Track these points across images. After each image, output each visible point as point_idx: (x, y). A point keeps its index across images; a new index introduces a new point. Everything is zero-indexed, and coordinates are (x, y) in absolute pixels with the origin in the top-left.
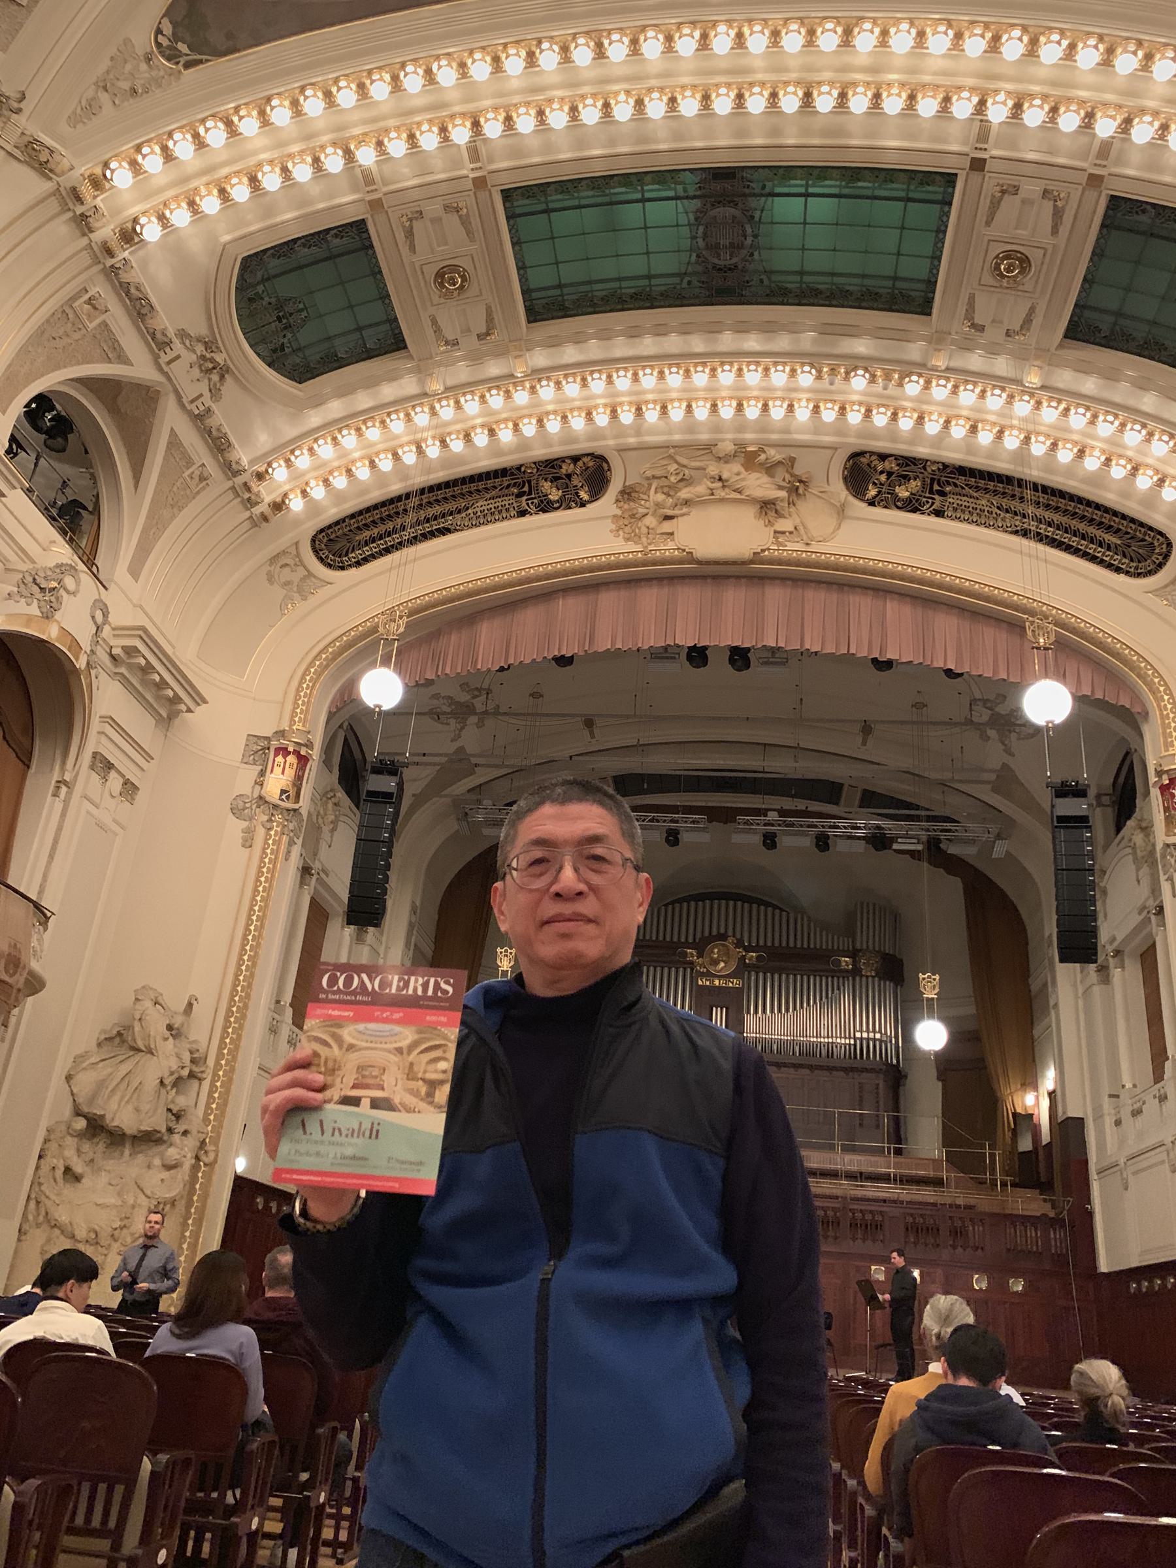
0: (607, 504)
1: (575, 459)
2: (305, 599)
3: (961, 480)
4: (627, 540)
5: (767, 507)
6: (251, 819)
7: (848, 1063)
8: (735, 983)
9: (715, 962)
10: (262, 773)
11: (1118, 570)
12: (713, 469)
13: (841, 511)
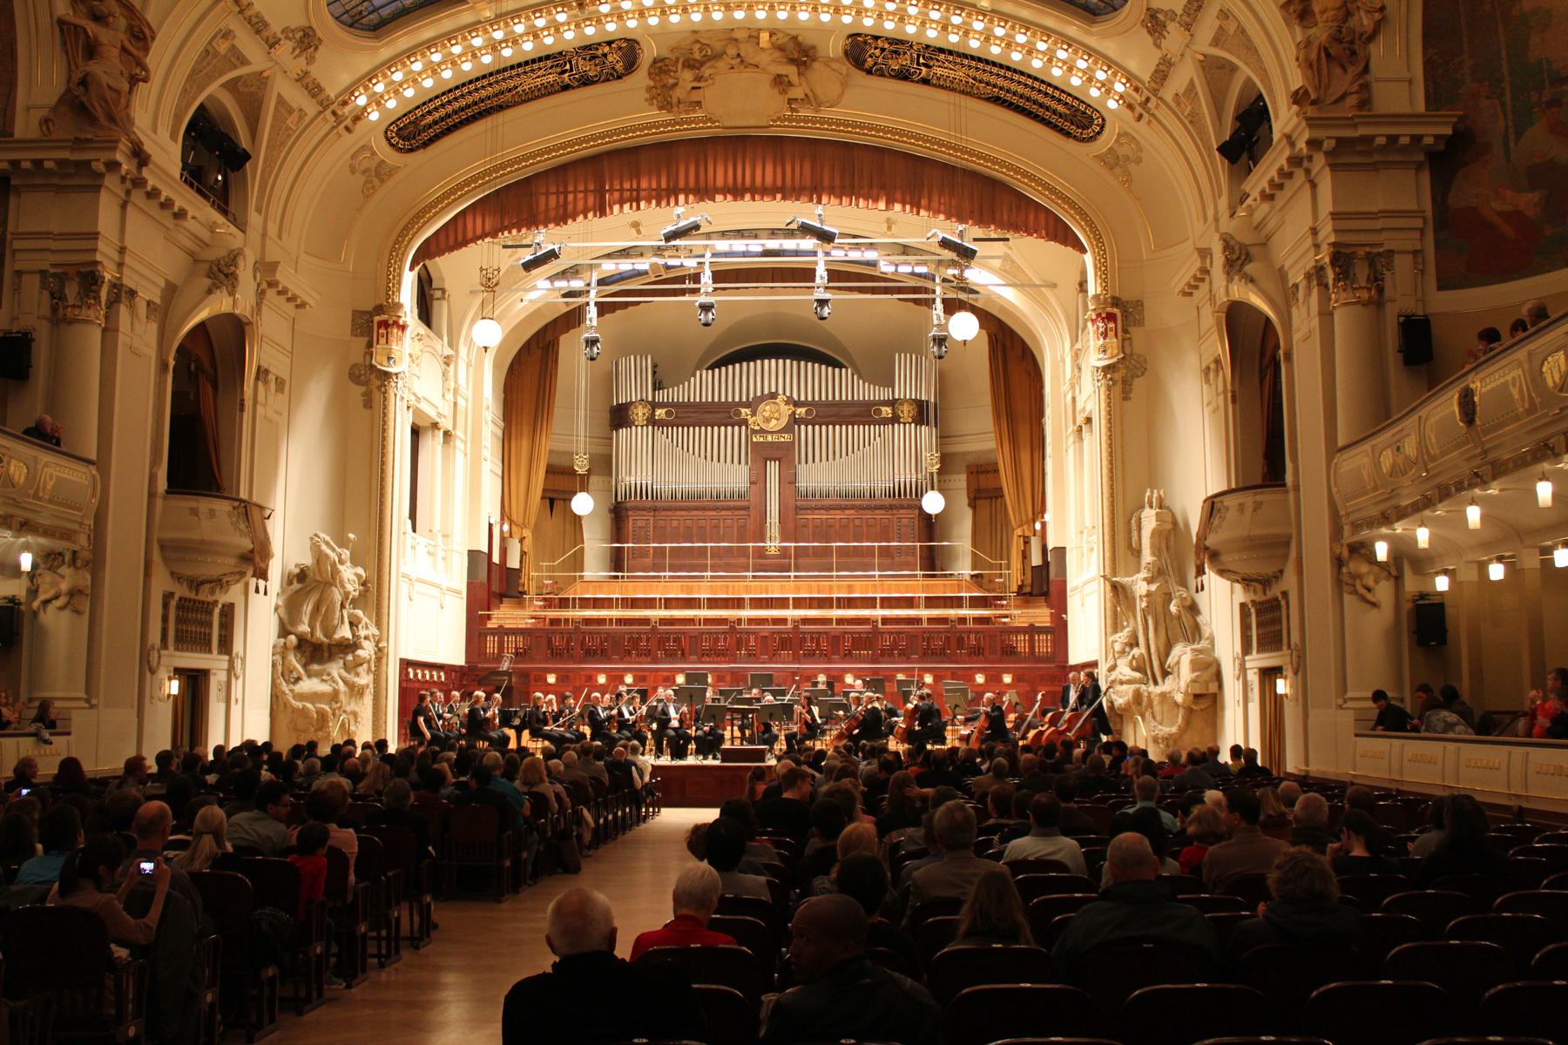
0: (640, 79)
1: (609, 43)
2: (382, 181)
3: (942, 57)
4: (661, 108)
5: (780, 82)
6: (367, 383)
7: (888, 501)
8: (786, 438)
9: (768, 420)
10: (370, 345)
11: (1068, 134)
12: (732, 51)
13: (845, 85)
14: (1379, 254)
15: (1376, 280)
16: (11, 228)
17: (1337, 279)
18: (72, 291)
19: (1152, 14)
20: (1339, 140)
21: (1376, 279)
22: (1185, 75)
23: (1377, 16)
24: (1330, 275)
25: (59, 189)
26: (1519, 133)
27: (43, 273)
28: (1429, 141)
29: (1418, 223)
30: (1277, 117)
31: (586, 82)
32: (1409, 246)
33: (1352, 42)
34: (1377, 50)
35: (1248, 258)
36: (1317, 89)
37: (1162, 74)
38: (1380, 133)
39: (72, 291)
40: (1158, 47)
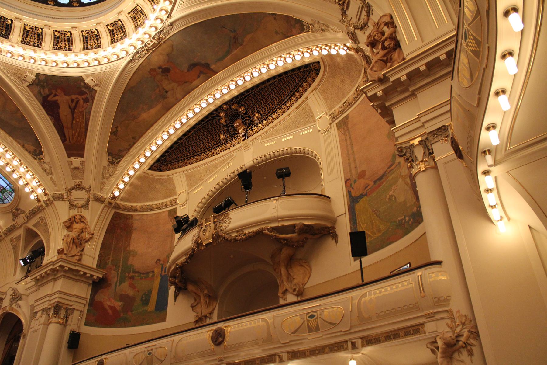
14: (70, 309)
15: (66, 317)
17: (54, 313)
19: (17, 209)
20: (69, 268)
21: (66, 317)
22: (21, 232)
23: (91, 236)
24: (52, 311)
26: (121, 283)
28: (95, 277)
29: (84, 302)
30: (48, 255)
32: (80, 309)
33: (81, 240)
34: (87, 245)
35: (21, 299)
36: (67, 251)
37: (10, 230)
38: (82, 270)
40: (14, 220)
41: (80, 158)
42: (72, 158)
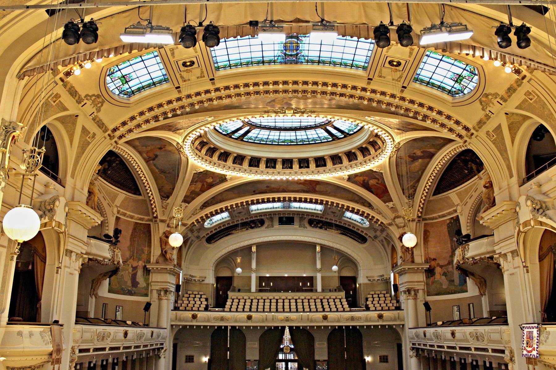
15: (416, 295)
16: (150, 280)
18: (162, 293)
25: (160, 273)
27: (157, 290)
31: (252, 228)
39: (162, 293)
41: (391, 203)
42: (387, 204)
